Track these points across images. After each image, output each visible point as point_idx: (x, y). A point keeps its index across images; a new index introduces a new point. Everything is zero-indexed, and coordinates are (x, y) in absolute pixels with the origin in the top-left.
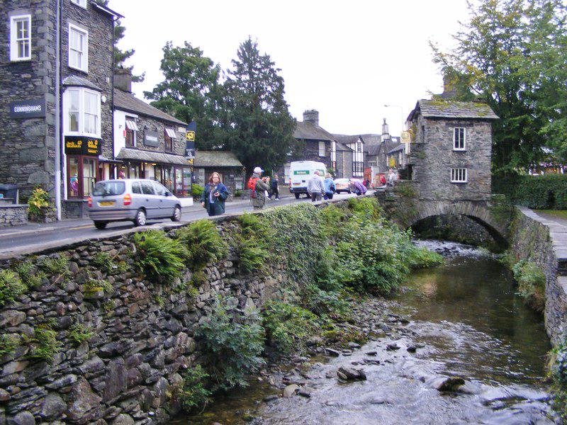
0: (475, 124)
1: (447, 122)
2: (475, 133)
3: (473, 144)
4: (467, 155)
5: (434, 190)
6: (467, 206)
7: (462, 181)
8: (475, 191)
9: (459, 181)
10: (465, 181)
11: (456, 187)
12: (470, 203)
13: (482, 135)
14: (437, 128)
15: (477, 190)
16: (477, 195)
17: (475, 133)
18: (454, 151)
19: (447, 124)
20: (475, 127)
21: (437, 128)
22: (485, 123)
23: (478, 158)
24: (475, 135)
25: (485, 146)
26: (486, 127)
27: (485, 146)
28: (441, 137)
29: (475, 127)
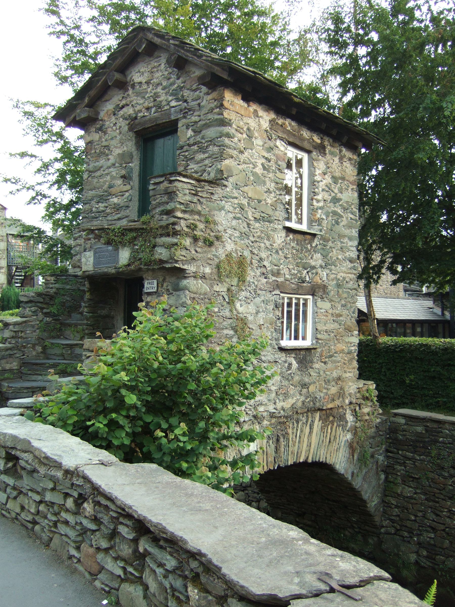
1: (272, 115)
7: (300, 343)
9: (293, 344)
10: (307, 343)
17: (328, 179)
20: (328, 157)
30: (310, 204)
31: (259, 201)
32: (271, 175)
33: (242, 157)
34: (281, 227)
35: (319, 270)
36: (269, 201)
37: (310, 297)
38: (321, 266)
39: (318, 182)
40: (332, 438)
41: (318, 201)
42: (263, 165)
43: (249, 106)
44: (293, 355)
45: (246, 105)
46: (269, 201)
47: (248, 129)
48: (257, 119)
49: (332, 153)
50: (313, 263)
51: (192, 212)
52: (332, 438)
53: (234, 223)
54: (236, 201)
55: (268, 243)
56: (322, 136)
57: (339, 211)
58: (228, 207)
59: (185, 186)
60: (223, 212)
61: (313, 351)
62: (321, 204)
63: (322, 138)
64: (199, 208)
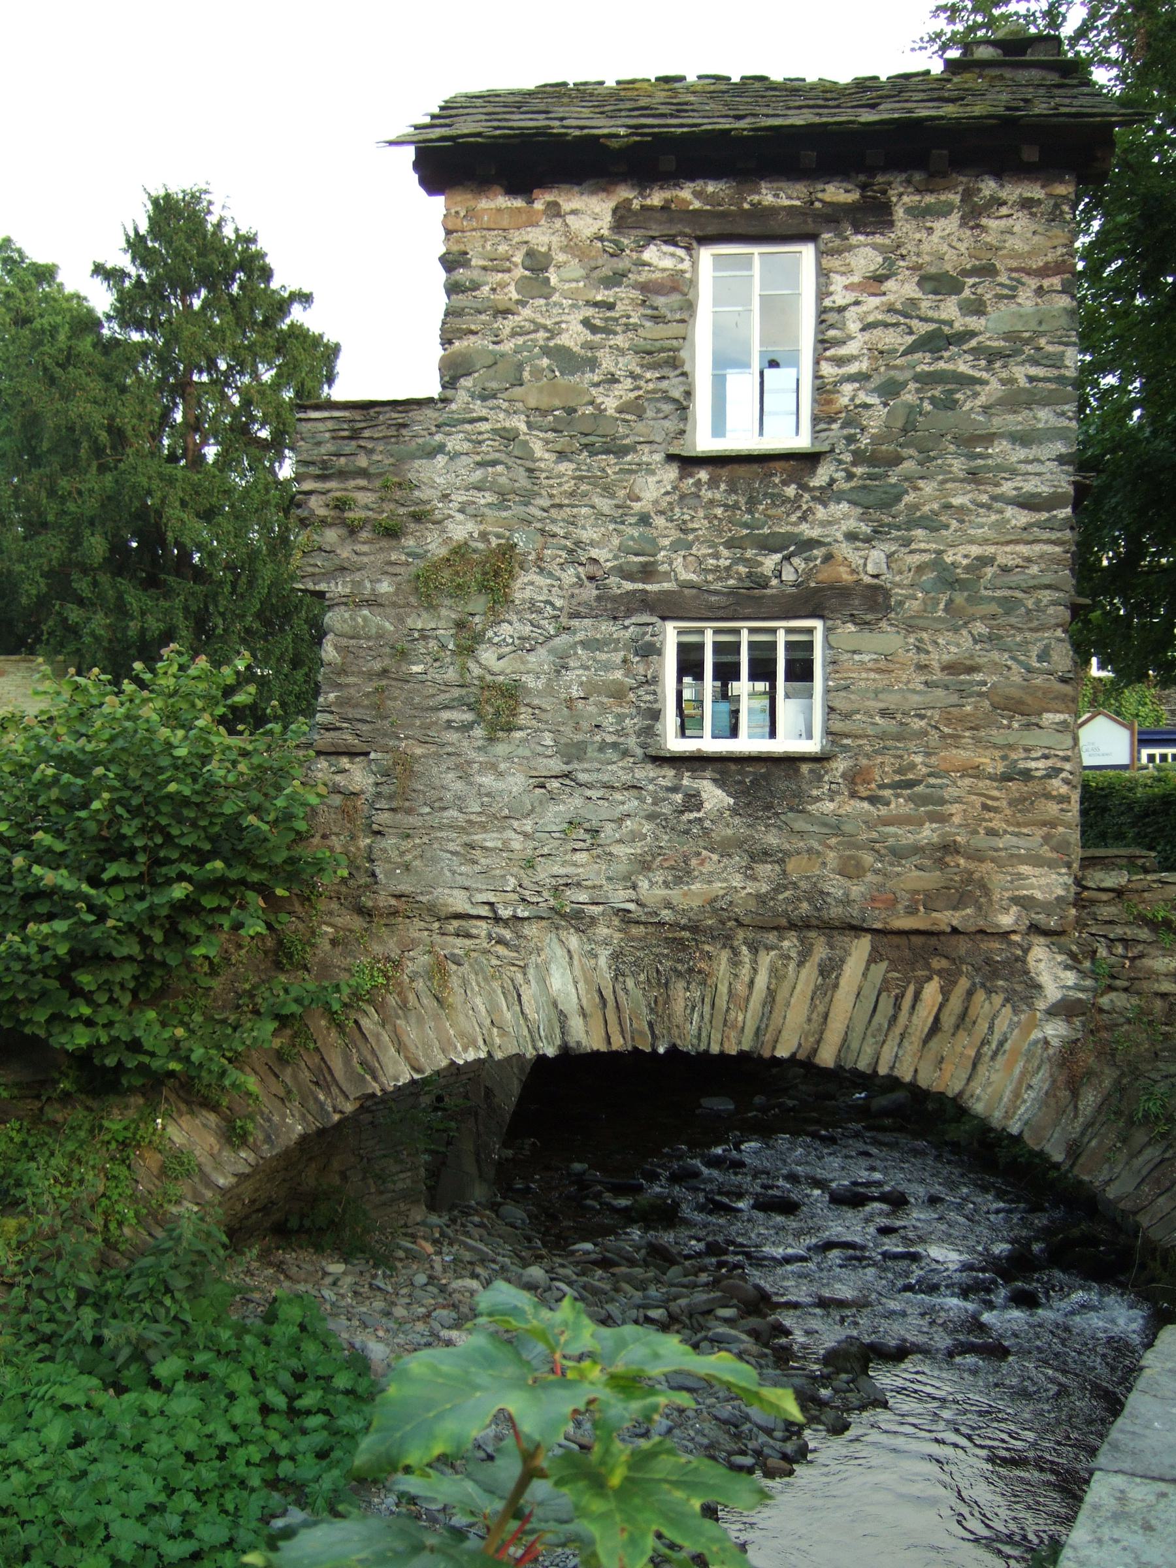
0: (903, 199)
2: (902, 288)
3: (890, 390)
4: (826, 495)
5: (502, 821)
6: (830, 970)
8: (904, 836)
10: (812, 746)
11: (714, 797)
12: (861, 947)
13: (977, 308)
14: (537, 263)
15: (928, 833)
16: (931, 879)
17: (902, 288)
18: (688, 463)
19: (623, 219)
21: (537, 263)
22: (1012, 192)
23: (932, 524)
24: (909, 310)
25: (1016, 400)
26: (1021, 223)
27: (1016, 400)
28: (573, 336)
29: (904, 227)
30: (817, 376)
31: (571, 411)
32: (620, 340)
33: (506, 325)
34: (658, 457)
35: (845, 550)
36: (610, 404)
37: (818, 624)
38: (851, 537)
39: (841, 310)
40: (948, 1021)
41: (840, 361)
42: (586, 323)
43: (530, 202)
44: (708, 774)
45: (519, 203)
46: (610, 404)
47: (530, 254)
48: (558, 223)
49: (918, 213)
50: (808, 531)
51: (343, 475)
52: (948, 1021)
53: (479, 474)
54: (484, 426)
55: (605, 504)
56: (862, 178)
57: (963, 367)
58: (455, 443)
59: (321, 426)
60: (441, 460)
61: (805, 768)
62: (853, 368)
63: (863, 187)
64: (362, 461)
